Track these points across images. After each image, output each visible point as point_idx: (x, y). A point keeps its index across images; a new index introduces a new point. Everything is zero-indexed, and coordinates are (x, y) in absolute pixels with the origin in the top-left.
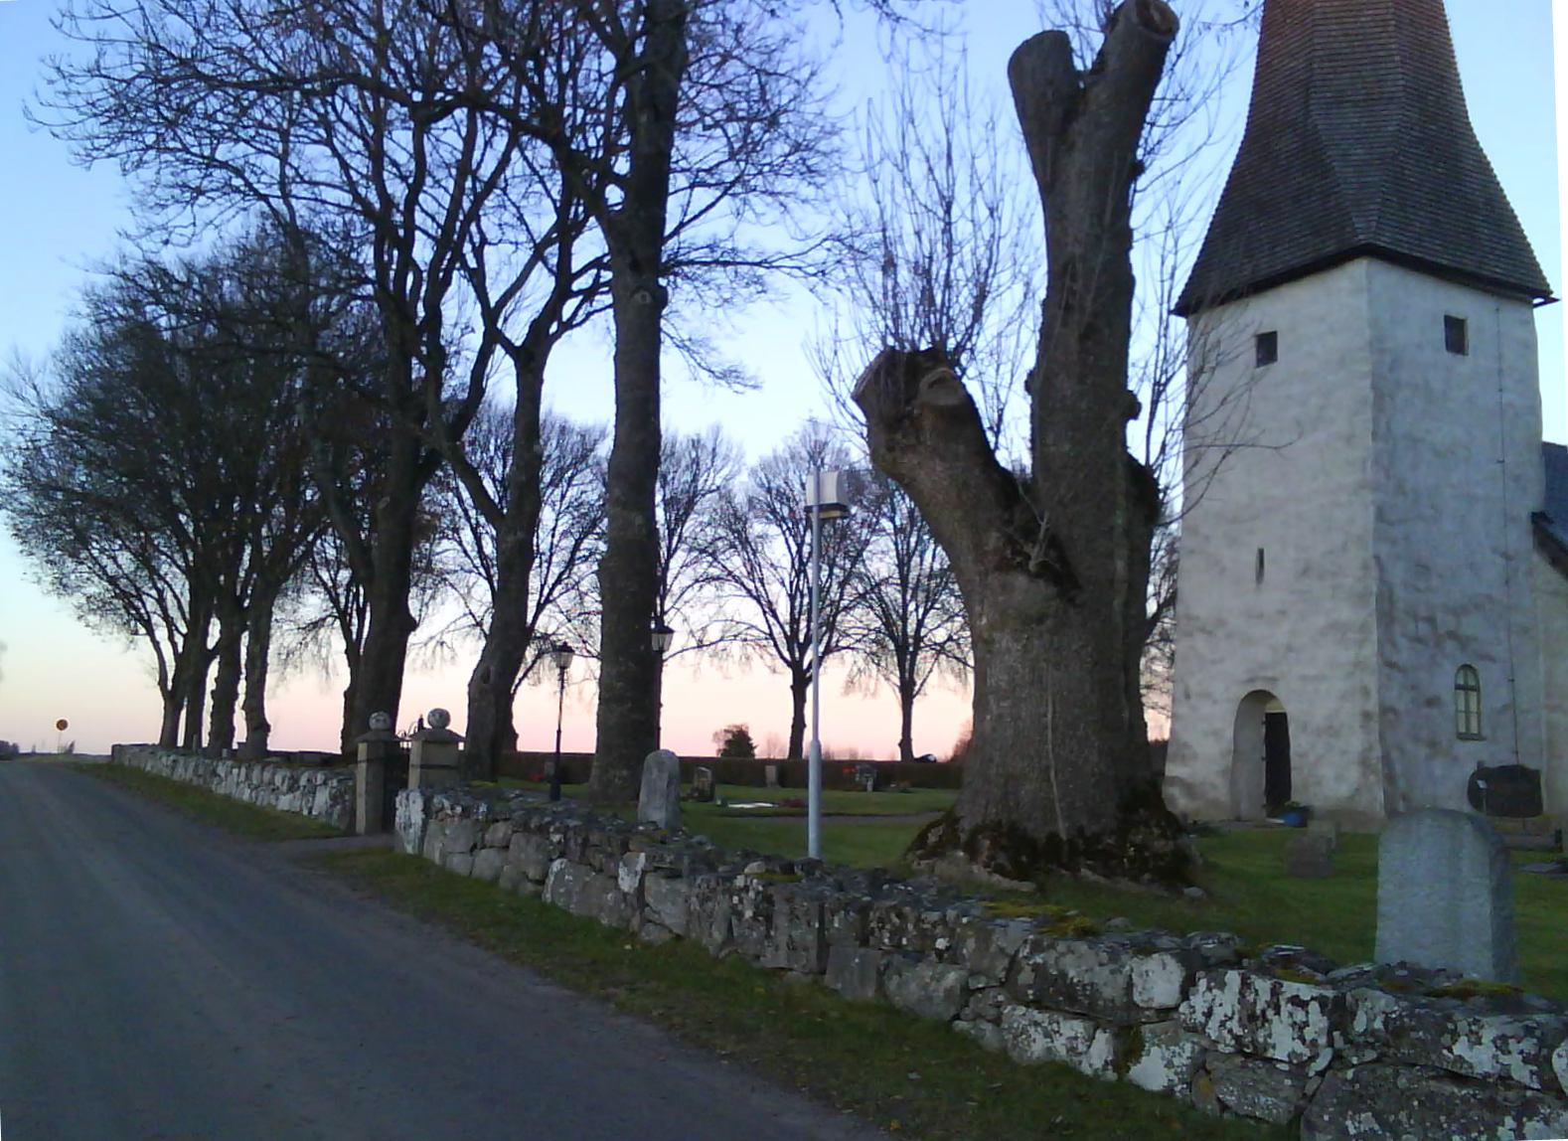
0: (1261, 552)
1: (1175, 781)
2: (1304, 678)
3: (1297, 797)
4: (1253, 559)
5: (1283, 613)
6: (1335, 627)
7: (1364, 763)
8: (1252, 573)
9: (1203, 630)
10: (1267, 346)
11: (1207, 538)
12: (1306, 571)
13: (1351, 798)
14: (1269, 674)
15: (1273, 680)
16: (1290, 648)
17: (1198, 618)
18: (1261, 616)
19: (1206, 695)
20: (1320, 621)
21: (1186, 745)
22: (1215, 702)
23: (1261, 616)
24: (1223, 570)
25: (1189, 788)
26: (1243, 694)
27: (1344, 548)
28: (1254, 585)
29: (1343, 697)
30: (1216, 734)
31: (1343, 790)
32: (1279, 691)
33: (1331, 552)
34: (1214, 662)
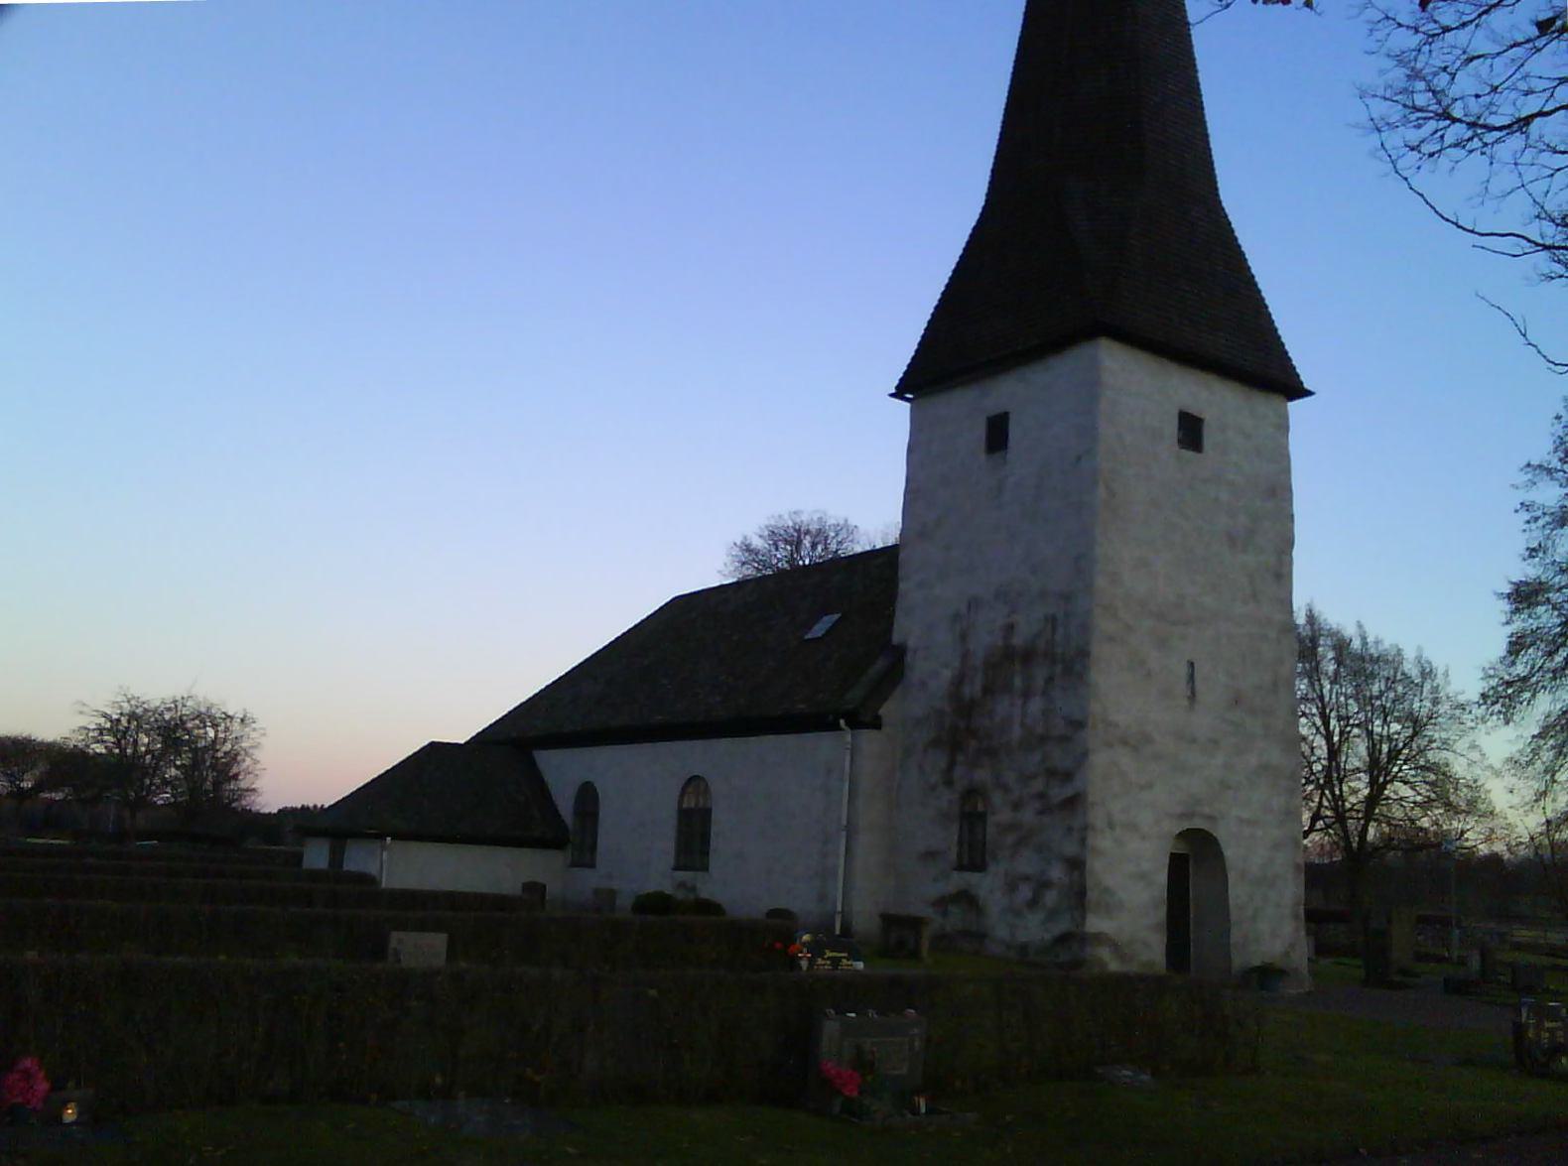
0: (1192, 665)
1: (1099, 938)
2: (1241, 820)
4: (1183, 671)
5: (1215, 742)
6: (1265, 768)
7: (1296, 917)
8: (1182, 687)
9: (1124, 742)
10: (1191, 431)
12: (1237, 701)
13: (1287, 954)
14: (1207, 810)
15: (1211, 818)
16: (1225, 786)
17: (1117, 725)
18: (1194, 741)
19: (1132, 827)
20: (1253, 760)
21: (1107, 890)
22: (1143, 838)
23: (1194, 741)
24: (1149, 674)
25: (1115, 947)
26: (1177, 832)
28: (1186, 703)
29: (1276, 846)
30: (1142, 876)
32: (1221, 833)
34: (1142, 788)
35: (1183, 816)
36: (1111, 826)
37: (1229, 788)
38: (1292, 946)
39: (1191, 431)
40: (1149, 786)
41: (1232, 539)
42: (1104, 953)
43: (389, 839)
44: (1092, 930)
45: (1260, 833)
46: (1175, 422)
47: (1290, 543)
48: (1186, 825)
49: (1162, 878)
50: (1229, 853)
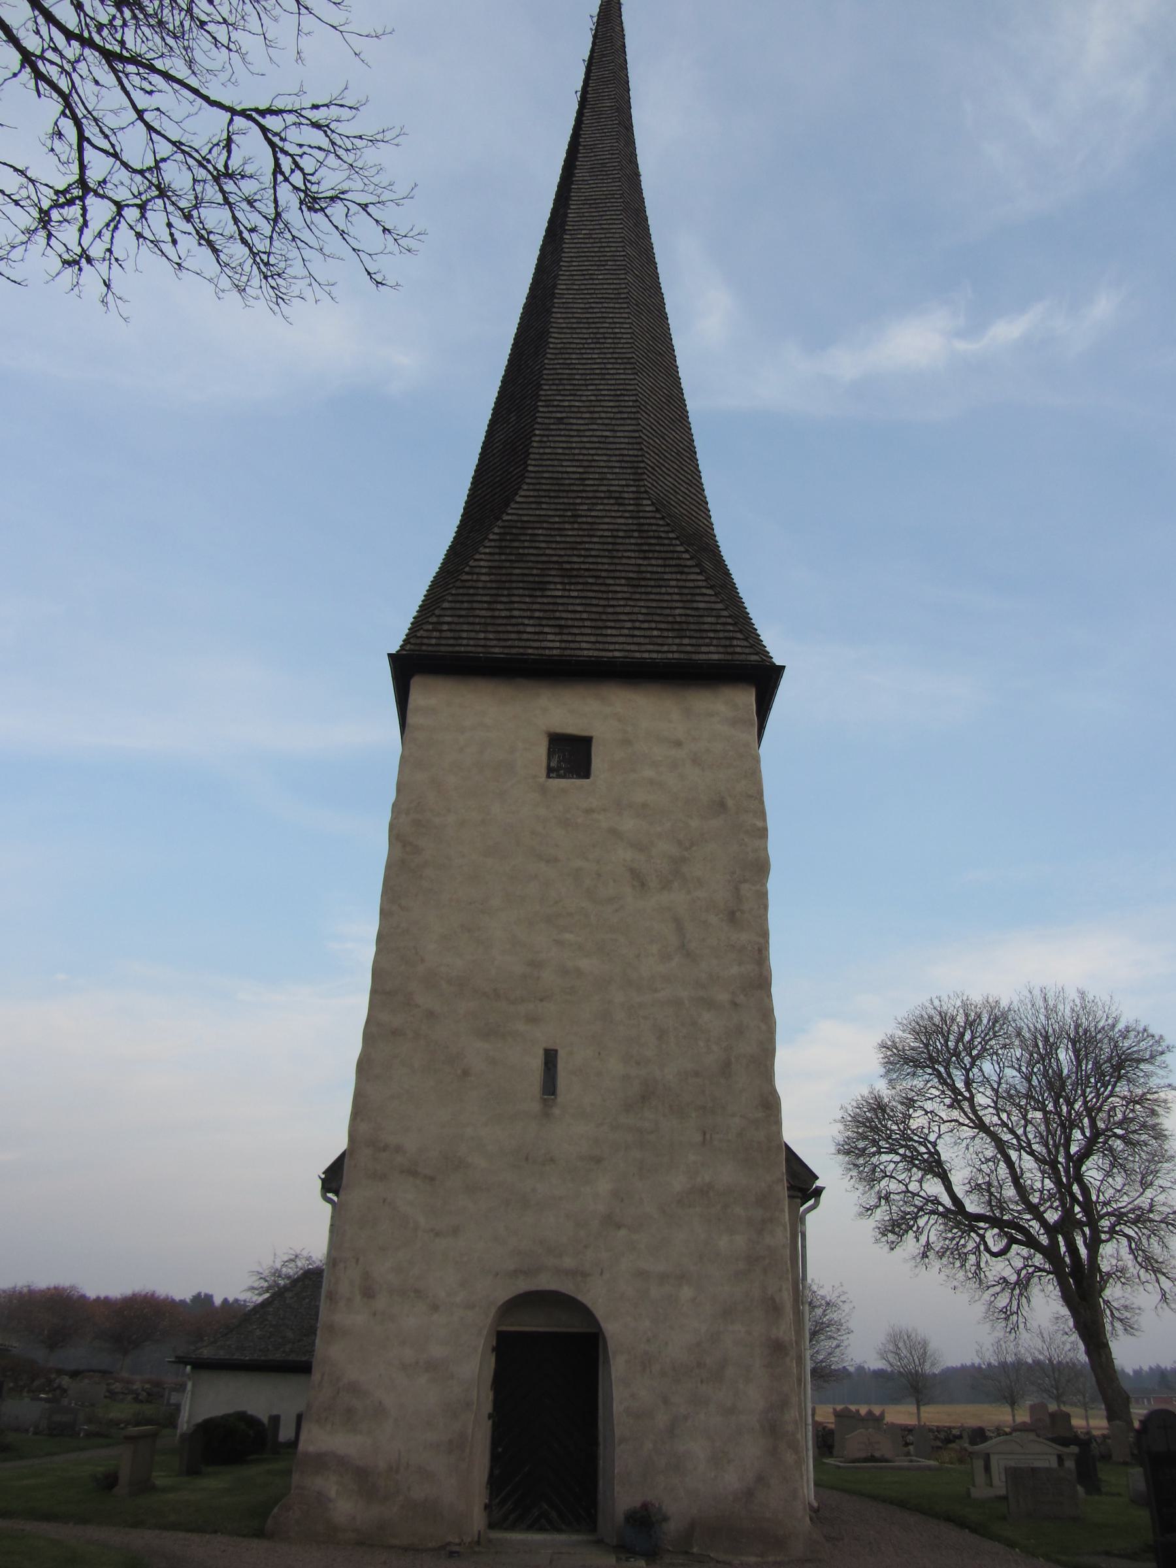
1: (321, 1462)
2: (642, 1274)
3: (622, 1496)
4: (536, 1062)
5: (598, 1160)
9: (411, 1172)
10: (571, 755)
11: (431, 1015)
12: (647, 1094)
13: (749, 1494)
14: (568, 1262)
15: (580, 1274)
16: (610, 1221)
17: (399, 1149)
20: (679, 1183)
21: (354, 1388)
22: (435, 1308)
24: (466, 1073)
26: (504, 1294)
27: (726, 1068)
28: (536, 1107)
31: (732, 1480)
32: (596, 1297)
33: (697, 1074)
35: (516, 1273)
36: (368, 1293)
37: (619, 1226)
38: (760, 1479)
39: (571, 755)
40: (455, 1231)
41: (638, 880)
42: (330, 1485)
43: (189, 1368)
44: (311, 1449)
45: (687, 1292)
46: (541, 750)
47: (761, 868)
48: (523, 1285)
49: (473, 1367)
50: (610, 1328)
